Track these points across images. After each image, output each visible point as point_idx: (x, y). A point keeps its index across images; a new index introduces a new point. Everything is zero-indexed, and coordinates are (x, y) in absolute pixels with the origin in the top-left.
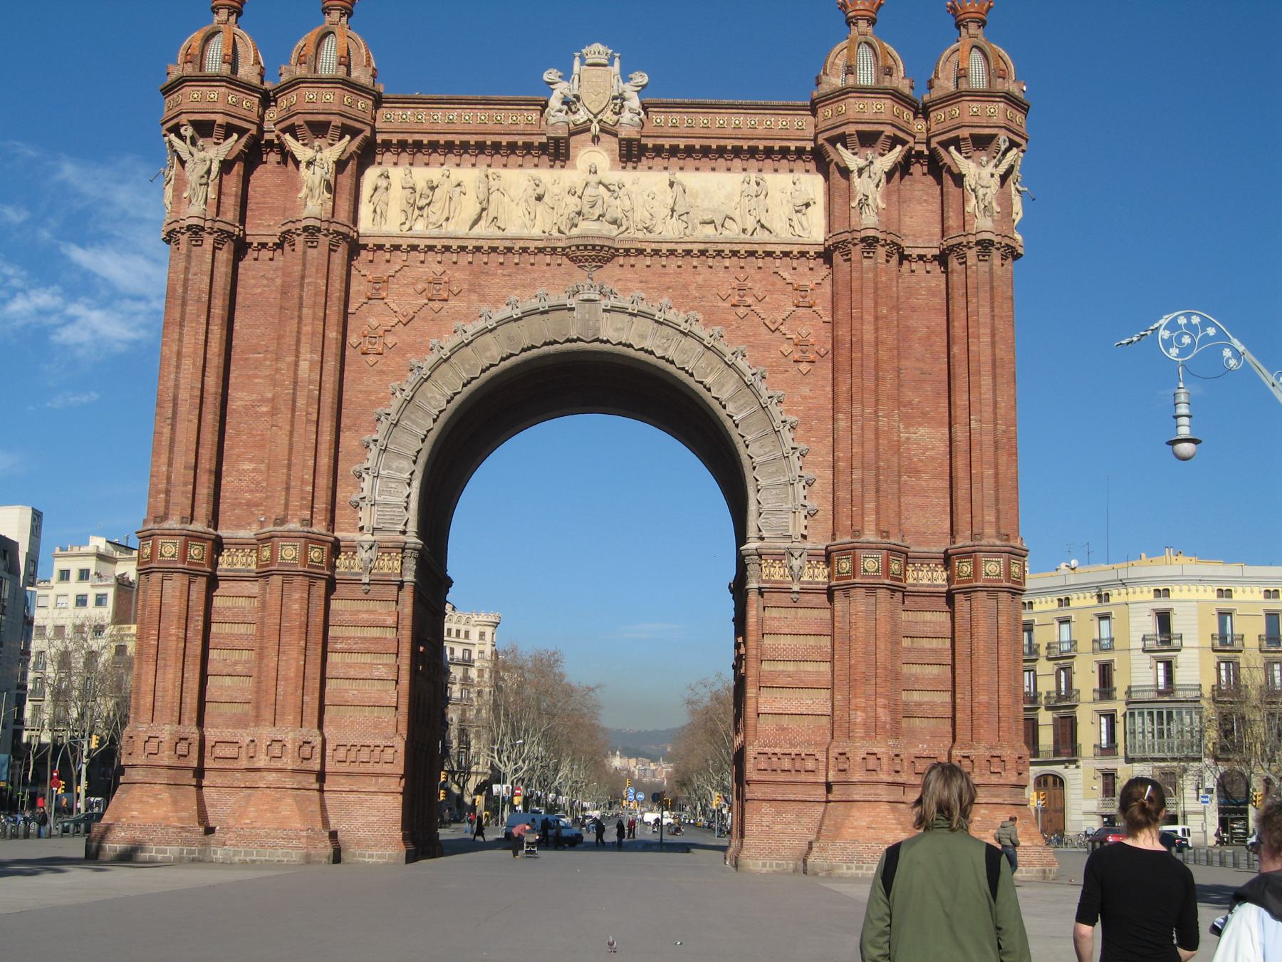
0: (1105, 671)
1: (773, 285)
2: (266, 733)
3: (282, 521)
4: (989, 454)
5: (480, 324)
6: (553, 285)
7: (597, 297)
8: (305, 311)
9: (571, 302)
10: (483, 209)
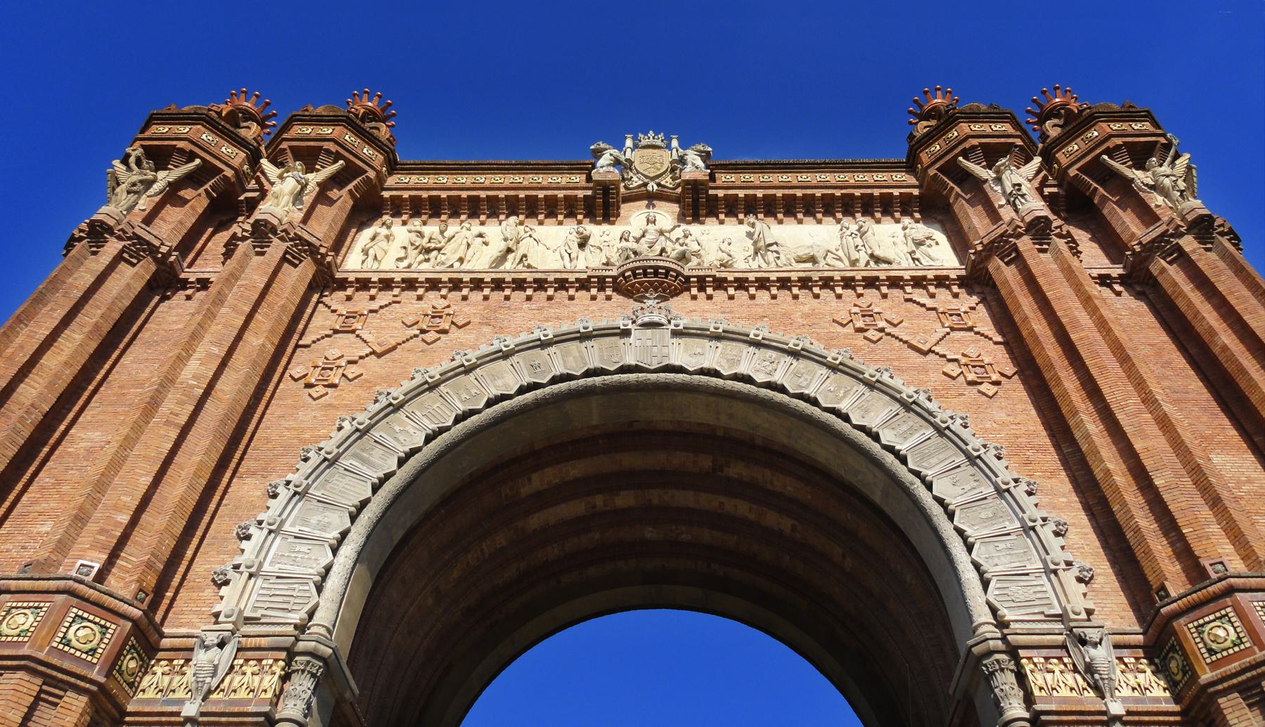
7: (664, 321)
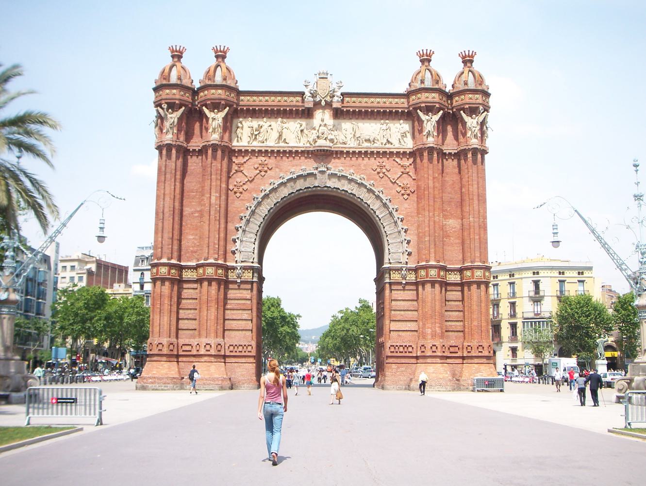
0: (513, 305)
1: (393, 164)
2: (204, 341)
3: (207, 259)
4: (477, 231)
5: (281, 181)
6: (308, 166)
8: (213, 176)
9: (315, 172)
10: (280, 135)
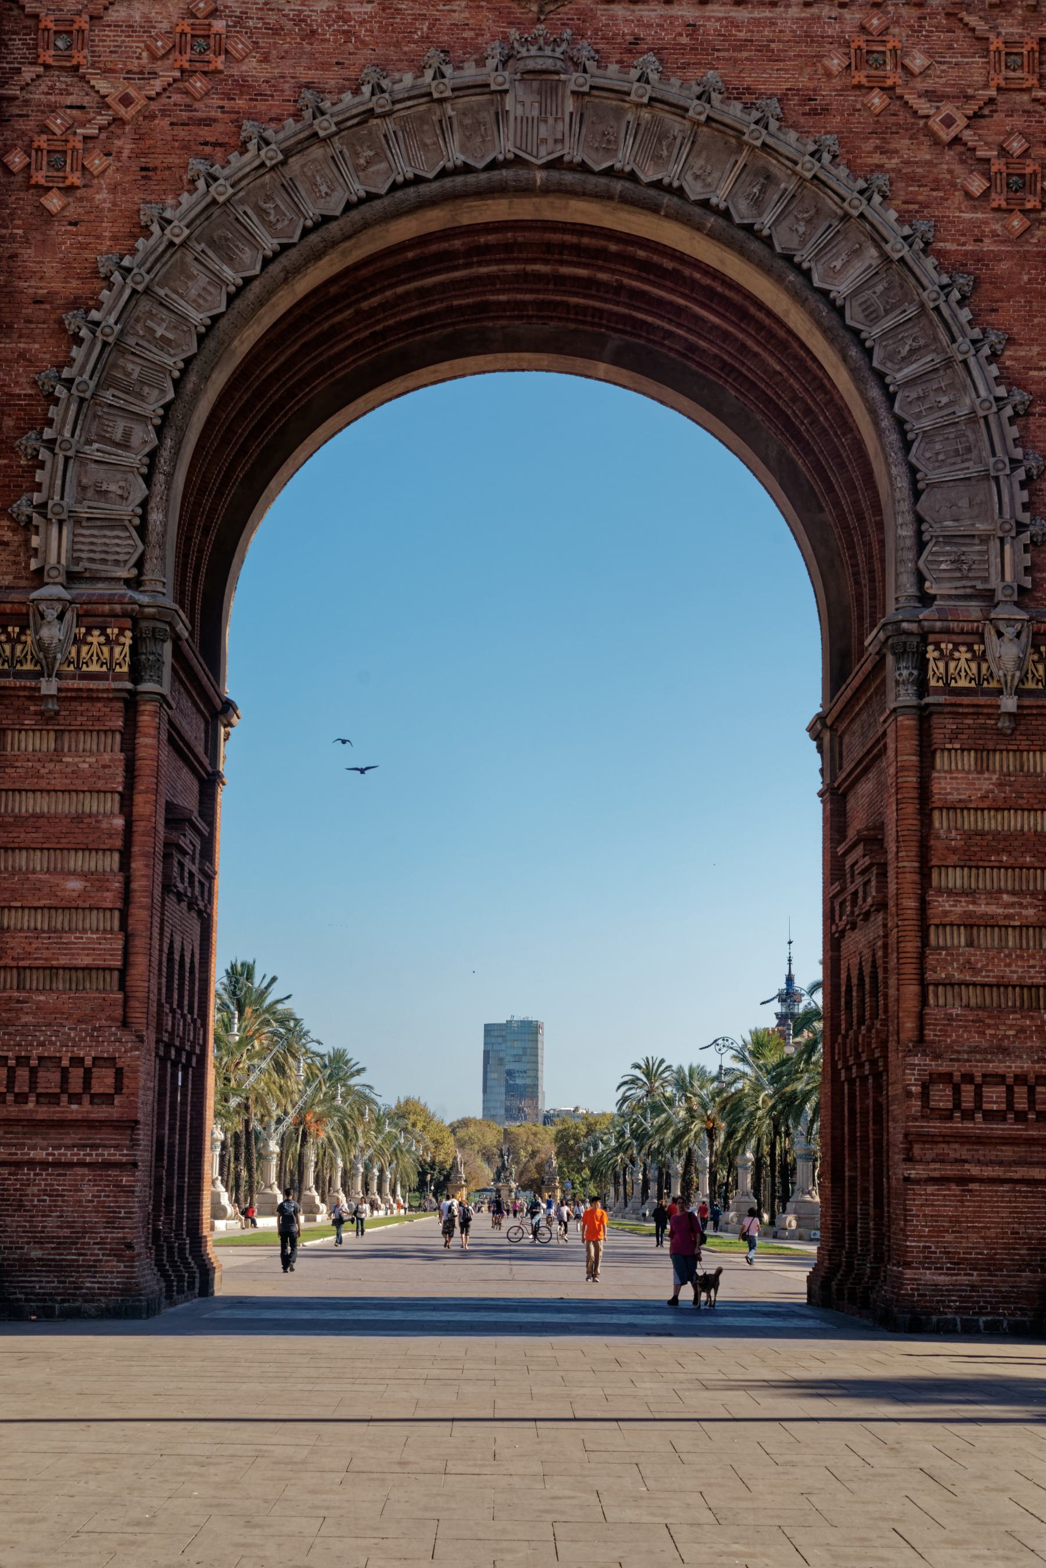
9: (498, 80)
